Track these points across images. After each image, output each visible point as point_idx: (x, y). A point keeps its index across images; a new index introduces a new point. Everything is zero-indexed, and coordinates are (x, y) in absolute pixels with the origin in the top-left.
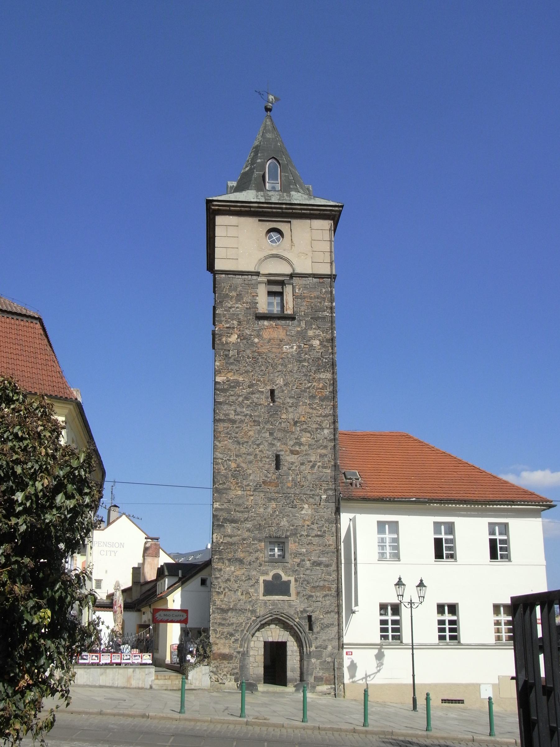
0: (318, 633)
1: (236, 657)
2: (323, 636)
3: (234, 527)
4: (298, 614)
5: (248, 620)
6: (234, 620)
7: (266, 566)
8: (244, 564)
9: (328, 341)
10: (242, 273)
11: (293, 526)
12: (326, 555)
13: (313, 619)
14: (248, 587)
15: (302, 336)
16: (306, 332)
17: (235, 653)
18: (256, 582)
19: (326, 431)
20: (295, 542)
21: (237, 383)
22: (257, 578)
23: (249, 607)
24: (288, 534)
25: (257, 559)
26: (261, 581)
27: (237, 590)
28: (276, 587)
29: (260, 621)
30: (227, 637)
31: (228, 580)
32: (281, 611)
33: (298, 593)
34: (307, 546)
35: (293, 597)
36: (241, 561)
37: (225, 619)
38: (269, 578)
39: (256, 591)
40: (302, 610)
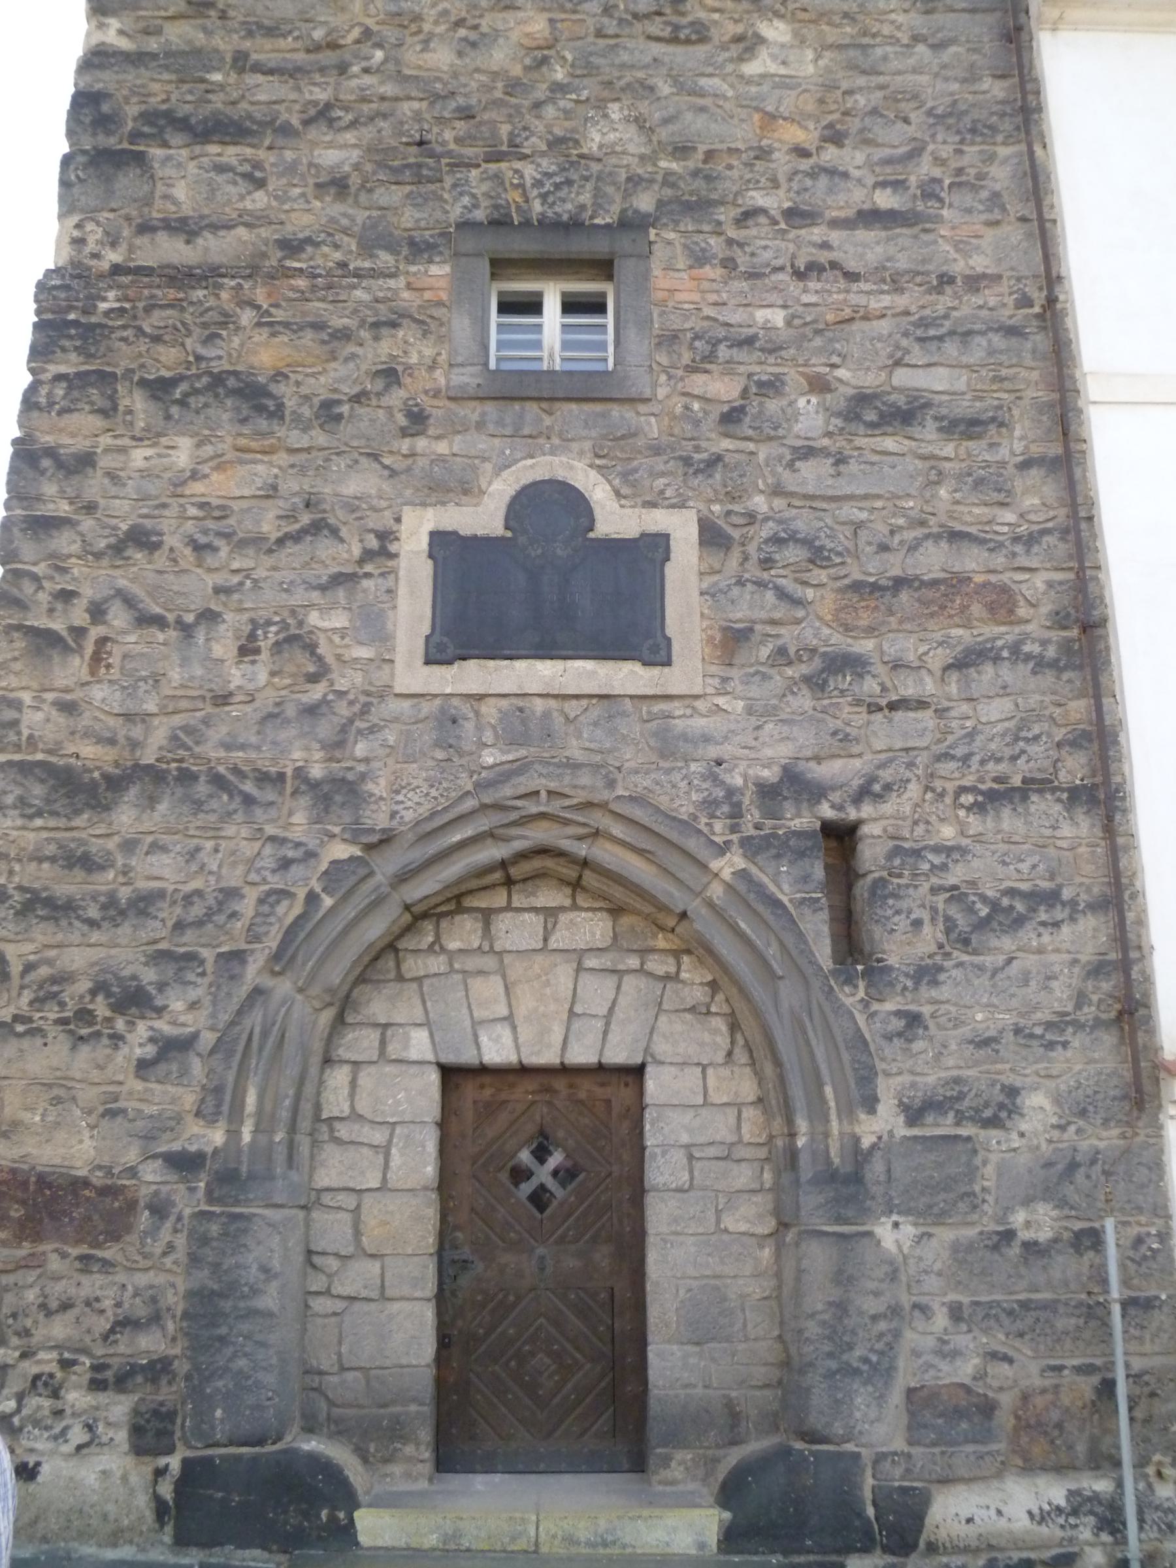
0: (927, 974)
1: (159, 1209)
2: (971, 1002)
3: (221, 169)
4: (736, 813)
5: (285, 864)
6: (162, 870)
7: (456, 428)
8: (278, 413)
11: (682, 151)
12: (951, 348)
13: (871, 854)
14: (300, 597)
17: (152, 1173)
18: (368, 555)
20: (700, 259)
22: (385, 521)
23: (304, 754)
24: (645, 202)
25: (390, 375)
26: (416, 531)
27: (209, 617)
28: (540, 588)
29: (404, 877)
30: (85, 1015)
31: (141, 539)
32: (587, 785)
33: (732, 640)
34: (794, 287)
35: (688, 672)
36: (255, 397)
37: (87, 863)
38: (484, 516)
39: (373, 625)
40: (770, 774)
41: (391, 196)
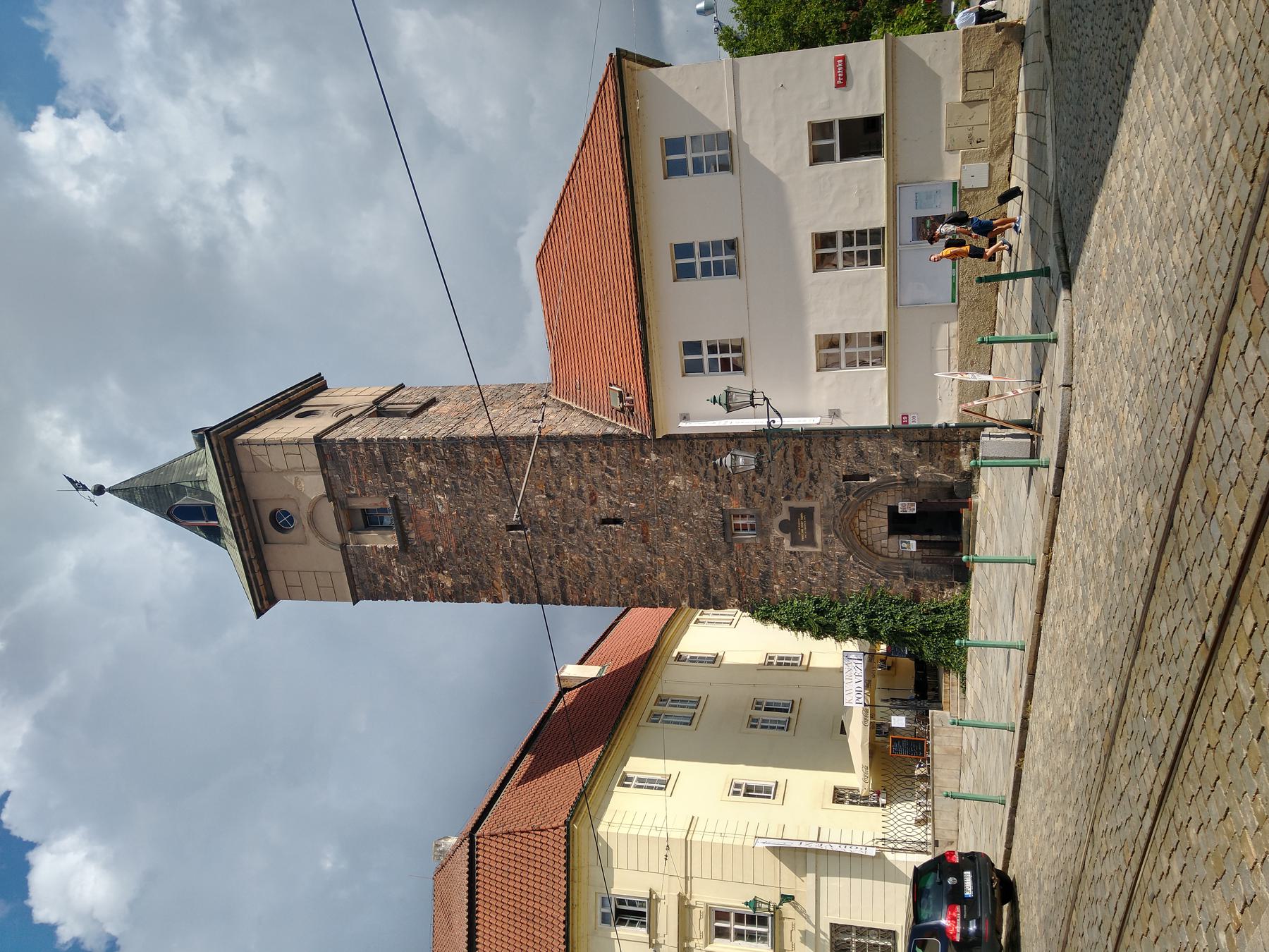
9: (417, 448)
10: (348, 568)
16: (413, 481)
19: (555, 454)
21: (508, 576)
33: (808, 496)
36: (766, 576)
39: (810, 554)
41: (719, 553)
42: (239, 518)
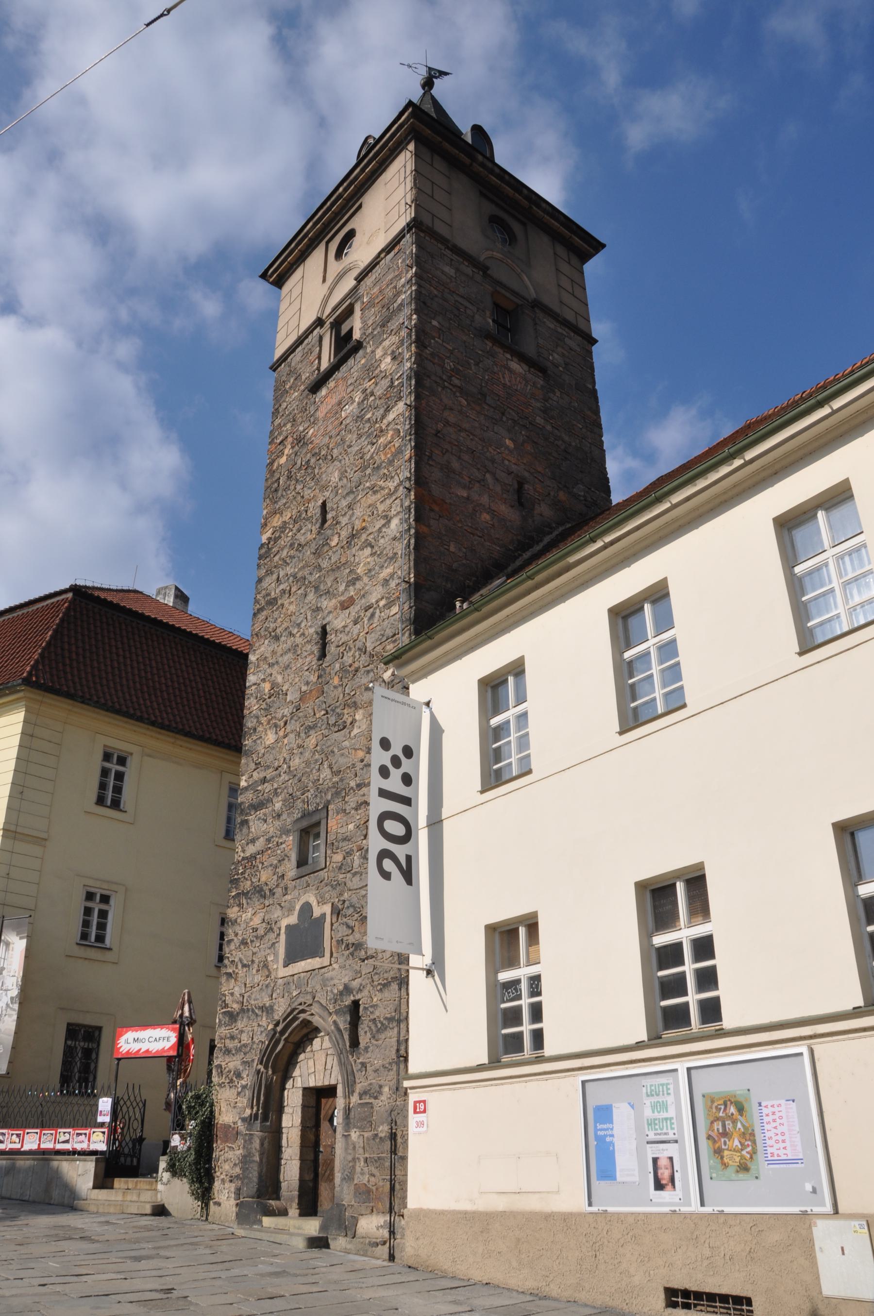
15: (370, 372)
21: (284, 527)
24: (329, 797)
36: (259, 891)
42: (340, 196)
